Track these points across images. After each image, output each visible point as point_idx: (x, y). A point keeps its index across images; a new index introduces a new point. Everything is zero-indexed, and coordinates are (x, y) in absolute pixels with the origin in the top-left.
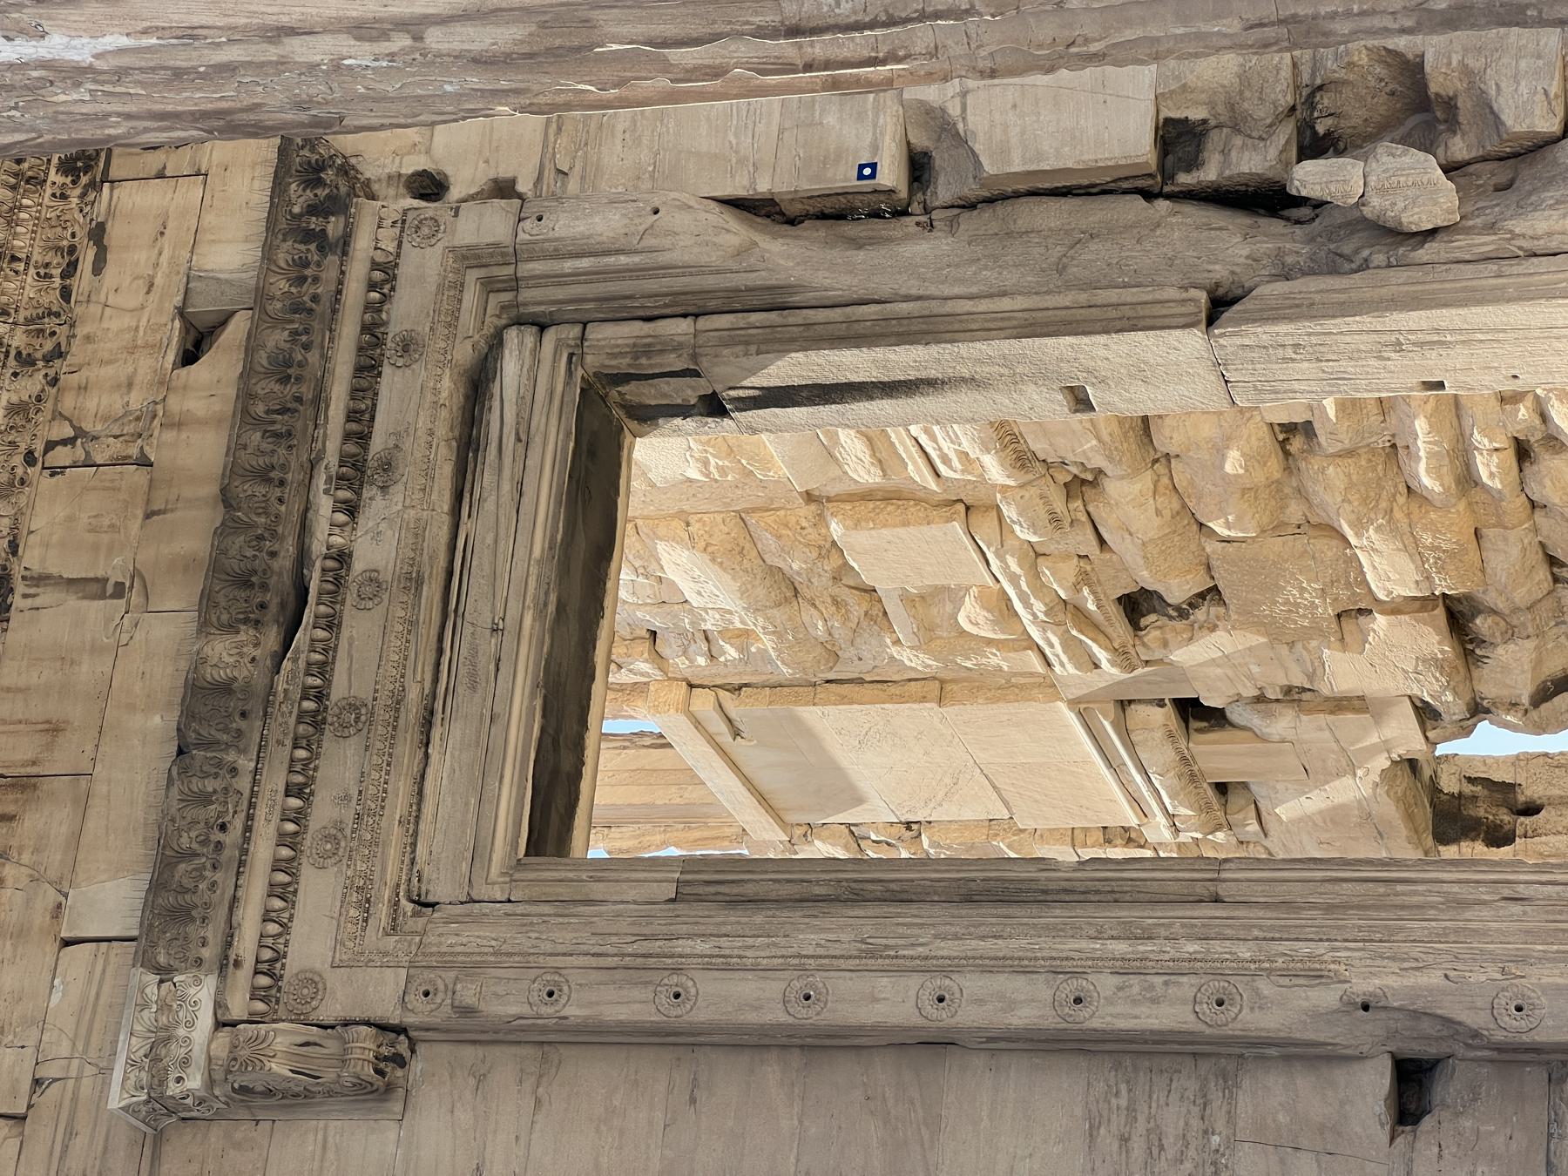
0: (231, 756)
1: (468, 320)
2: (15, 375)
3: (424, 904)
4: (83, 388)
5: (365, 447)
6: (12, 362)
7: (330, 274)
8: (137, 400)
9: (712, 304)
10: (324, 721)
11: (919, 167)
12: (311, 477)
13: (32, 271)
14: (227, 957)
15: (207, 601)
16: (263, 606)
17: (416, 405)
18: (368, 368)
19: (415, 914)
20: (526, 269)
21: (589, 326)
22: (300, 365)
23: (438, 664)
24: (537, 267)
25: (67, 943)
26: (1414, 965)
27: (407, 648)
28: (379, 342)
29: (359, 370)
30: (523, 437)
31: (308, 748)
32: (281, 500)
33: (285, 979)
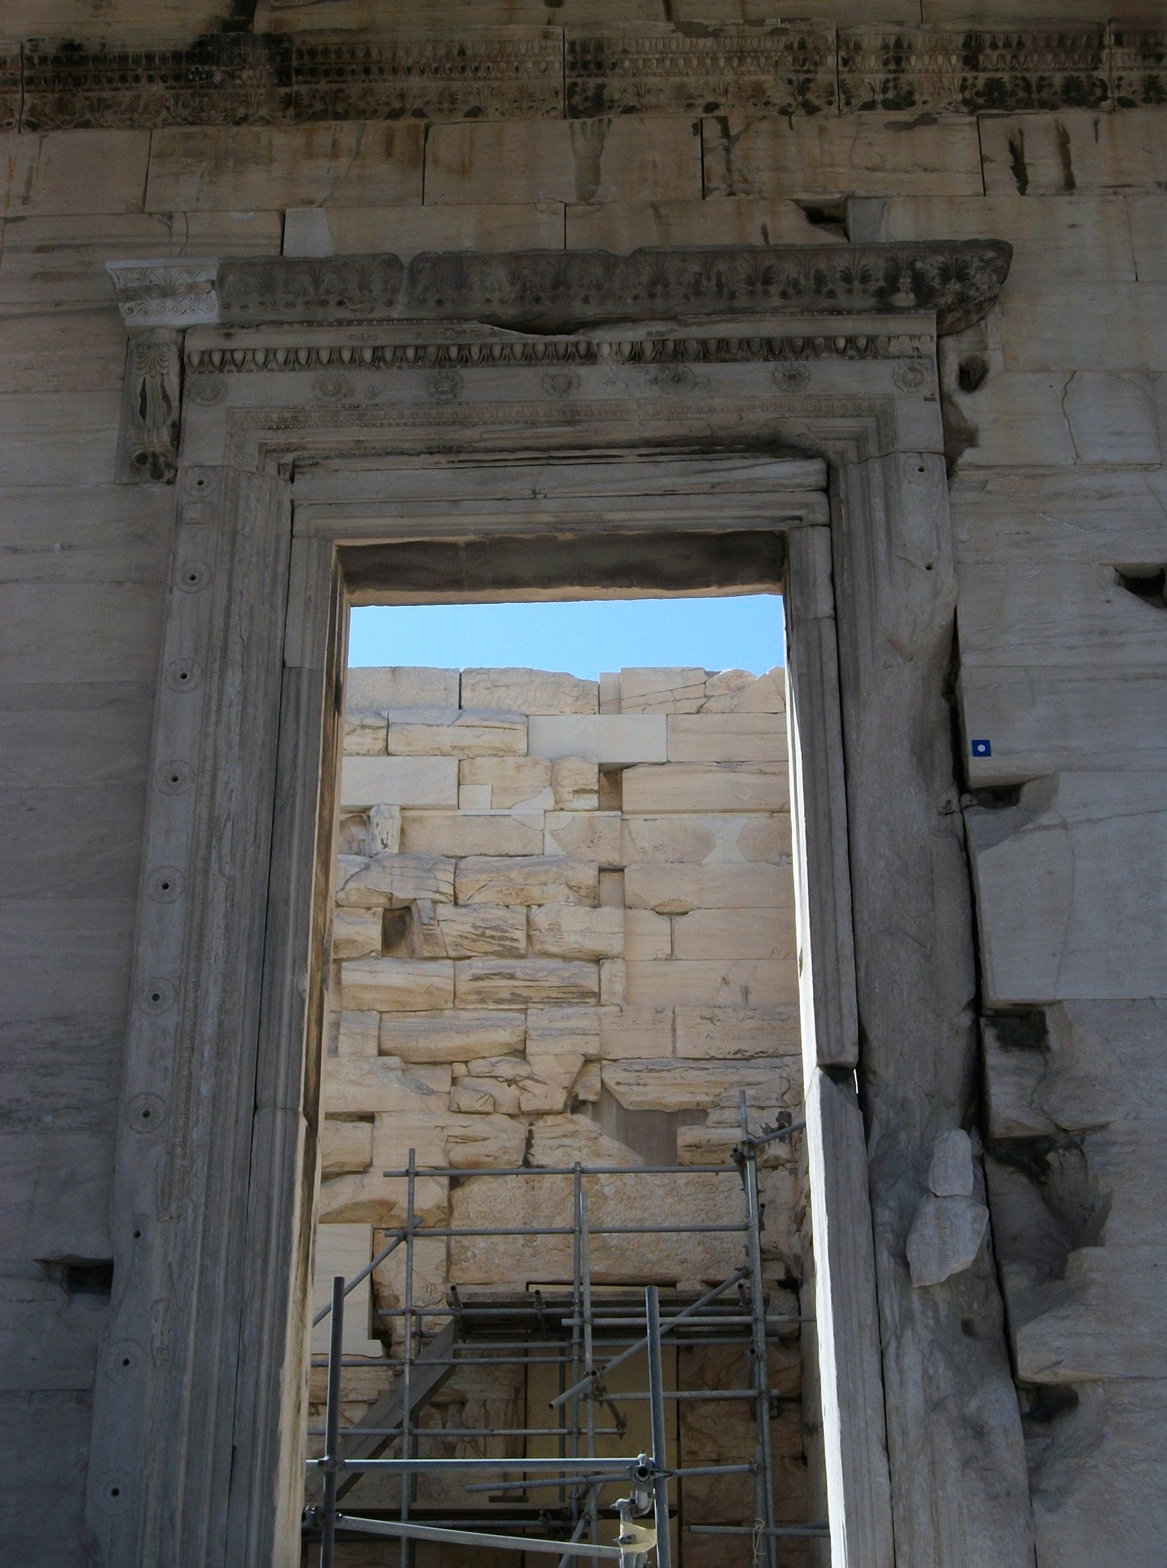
0: (402, 298)
1: (827, 423)
2: (790, 82)
3: (293, 472)
4: (776, 135)
5: (697, 359)
6: (802, 77)
7: (857, 302)
8: (764, 178)
9: (844, 628)
10: (442, 367)
11: (1004, 795)
12: (663, 320)
13: (891, 76)
14: (232, 326)
15: (537, 255)
16: (538, 300)
17: (743, 393)
18: (771, 349)
19: (280, 468)
20: (876, 467)
21: (826, 530)
22: (766, 292)
23: (502, 450)
24: (876, 475)
26: (175, 1275)
27: (509, 422)
28: (799, 353)
29: (768, 343)
30: (716, 490)
31: (417, 358)
32: (635, 298)
33: (221, 375)
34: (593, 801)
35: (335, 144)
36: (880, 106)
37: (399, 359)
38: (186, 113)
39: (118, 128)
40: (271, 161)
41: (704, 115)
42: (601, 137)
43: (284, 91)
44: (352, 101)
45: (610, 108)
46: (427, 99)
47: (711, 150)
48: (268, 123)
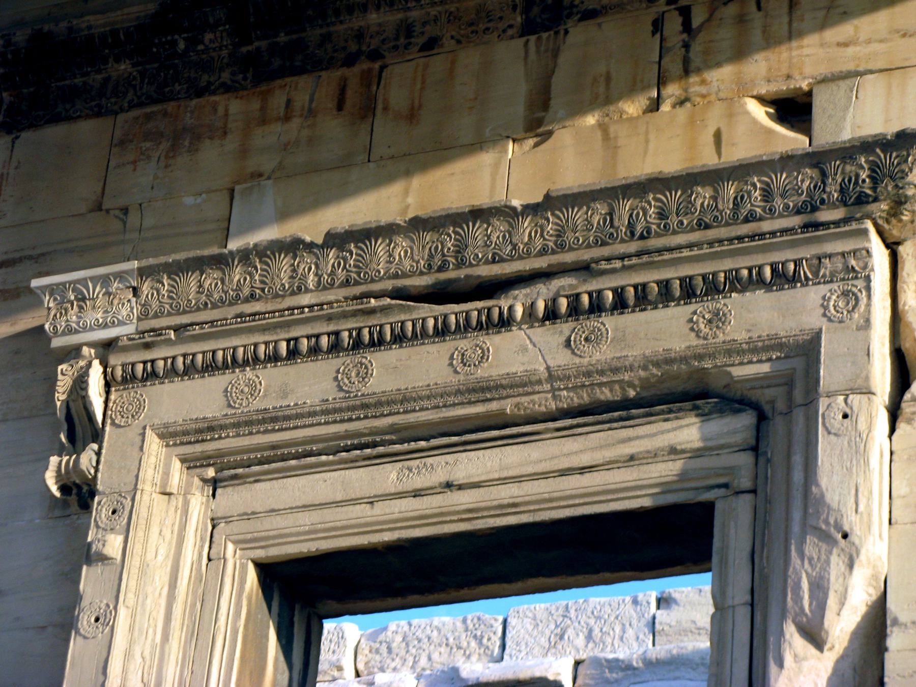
9: (758, 618)
20: (799, 415)
35: (289, 103)
37: (315, 351)
41: (666, 8)
42: (556, 53)
45: (569, 16)
46: (384, 37)
47: (669, 50)
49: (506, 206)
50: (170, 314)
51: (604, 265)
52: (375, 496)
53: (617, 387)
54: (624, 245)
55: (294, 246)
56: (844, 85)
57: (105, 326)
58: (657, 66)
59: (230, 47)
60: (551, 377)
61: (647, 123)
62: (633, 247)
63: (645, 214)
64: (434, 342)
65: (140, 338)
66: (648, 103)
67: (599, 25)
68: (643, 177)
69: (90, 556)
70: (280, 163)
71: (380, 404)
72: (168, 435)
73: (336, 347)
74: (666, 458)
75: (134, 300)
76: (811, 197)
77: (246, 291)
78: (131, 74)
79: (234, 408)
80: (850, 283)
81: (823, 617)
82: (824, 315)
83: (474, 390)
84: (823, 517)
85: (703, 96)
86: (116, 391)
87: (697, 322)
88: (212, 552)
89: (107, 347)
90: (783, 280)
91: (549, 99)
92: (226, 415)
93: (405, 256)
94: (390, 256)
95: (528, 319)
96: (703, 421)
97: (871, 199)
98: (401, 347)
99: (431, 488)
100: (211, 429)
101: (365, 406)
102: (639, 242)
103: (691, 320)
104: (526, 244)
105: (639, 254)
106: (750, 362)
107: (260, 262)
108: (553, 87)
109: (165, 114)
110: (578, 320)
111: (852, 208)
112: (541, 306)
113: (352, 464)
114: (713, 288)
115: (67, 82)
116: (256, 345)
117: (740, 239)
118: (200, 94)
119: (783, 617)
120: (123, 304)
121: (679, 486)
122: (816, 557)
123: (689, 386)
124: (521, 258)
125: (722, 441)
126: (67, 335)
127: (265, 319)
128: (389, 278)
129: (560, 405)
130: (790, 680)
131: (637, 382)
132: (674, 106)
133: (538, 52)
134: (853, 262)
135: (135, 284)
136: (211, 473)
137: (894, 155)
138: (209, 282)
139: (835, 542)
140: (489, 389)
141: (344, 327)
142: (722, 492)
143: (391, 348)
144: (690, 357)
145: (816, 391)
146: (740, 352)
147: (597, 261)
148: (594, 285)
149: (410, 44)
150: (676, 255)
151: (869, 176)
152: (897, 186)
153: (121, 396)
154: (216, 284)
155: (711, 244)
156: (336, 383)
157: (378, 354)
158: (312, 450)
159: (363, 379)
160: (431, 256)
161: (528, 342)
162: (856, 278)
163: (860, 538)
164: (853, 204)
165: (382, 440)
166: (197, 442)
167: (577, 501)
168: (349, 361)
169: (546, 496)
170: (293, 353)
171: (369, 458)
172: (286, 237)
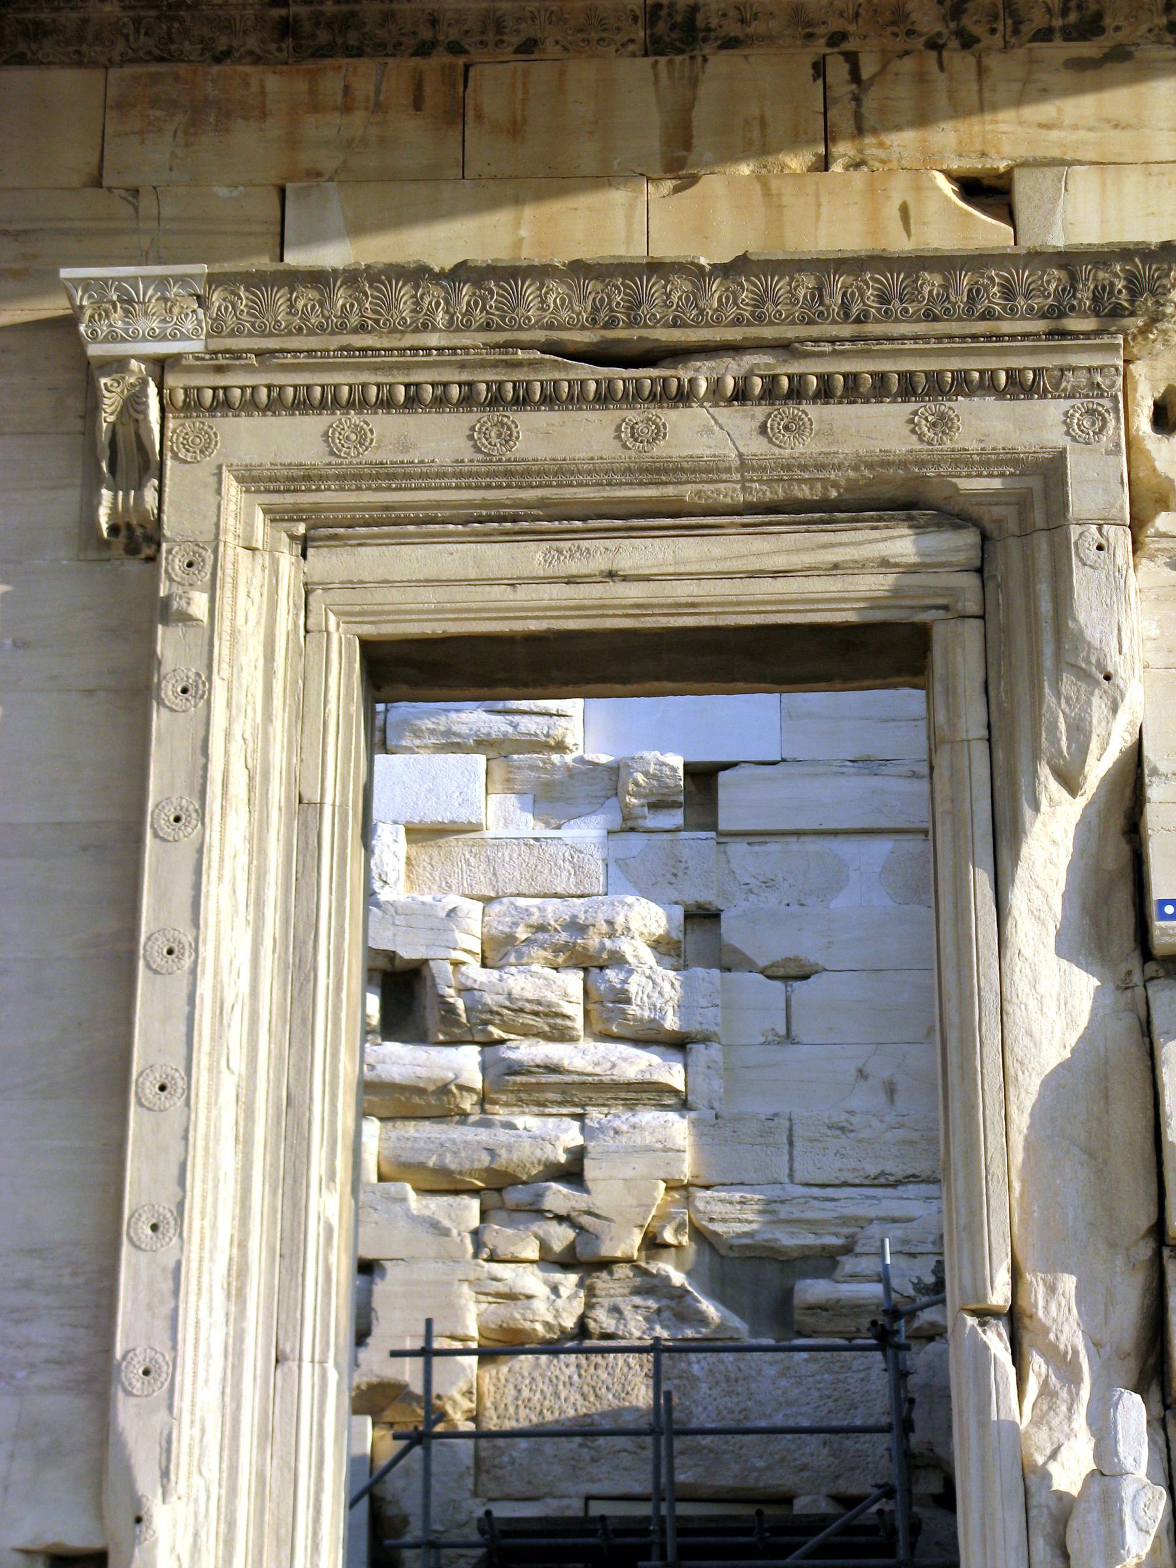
4: (921, 78)
9: (999, 755)
20: (1042, 543)
21: (977, 623)
25: (282, 192)
34: (676, 818)
35: (347, 90)
36: (1058, 35)
37: (441, 402)
38: (151, 42)
39: (63, 65)
40: (264, 116)
41: (828, 50)
42: (694, 83)
43: (277, 13)
44: (368, 29)
45: (705, 40)
46: (466, 27)
47: (836, 101)
48: (257, 60)
49: (692, 264)
50: (250, 335)
51: (809, 347)
52: (518, 578)
53: (819, 485)
54: (836, 327)
55: (418, 274)
56: (1050, 173)
57: (163, 338)
58: (821, 118)
59: (257, 7)
60: (744, 464)
61: (817, 183)
62: (847, 330)
63: (862, 295)
64: (594, 409)
65: (211, 359)
66: (814, 159)
67: (746, 57)
68: (863, 253)
69: (167, 612)
70: (344, 163)
71: (528, 473)
72: (250, 479)
73: (468, 400)
74: (874, 571)
75: (200, 311)
76: (1059, 302)
77: (354, 320)
78: (119, 19)
79: (340, 457)
80: (1095, 401)
81: (1084, 761)
82: (1068, 433)
83: (648, 471)
84: (1083, 654)
85: (883, 162)
86: (174, 418)
87: (918, 425)
88: (309, 622)
89: (161, 366)
90: (1017, 389)
91: (691, 137)
92: (330, 464)
93: (562, 305)
94: (542, 302)
95: (711, 396)
96: (917, 534)
97: (1127, 313)
98: (552, 409)
99: (590, 576)
100: (307, 478)
101: (508, 473)
102: (854, 326)
103: (912, 421)
104: (716, 310)
105: (853, 340)
106: (980, 475)
107: (371, 287)
108: (695, 123)
109: (177, 78)
110: (773, 404)
111: (1104, 319)
112: (730, 383)
113: (485, 538)
114: (936, 386)
115: (30, 15)
116: (364, 386)
117: (974, 337)
118: (219, 58)
119: (1035, 757)
120: (187, 315)
121: (891, 602)
122: (1074, 697)
123: (901, 494)
124: (708, 325)
125: (944, 559)
126: (110, 342)
127: (379, 356)
128: (542, 328)
129: (749, 498)
130: (1044, 825)
131: (843, 483)
132: (847, 168)
133: (671, 77)
134: (1099, 379)
135: (200, 292)
136: (301, 529)
137: (1154, 267)
138: (302, 303)
139: (1097, 683)
140: (666, 471)
141: (481, 378)
142: (941, 614)
143: (539, 410)
144: (911, 463)
145: (1065, 517)
146: (969, 463)
147: (802, 341)
148: (795, 368)
149: (502, 41)
150: (897, 346)
151: (1124, 287)
152: (1157, 302)
153: (183, 425)
154: (313, 307)
155: (939, 339)
156: (472, 443)
157: (523, 415)
158: (436, 515)
159: (507, 442)
160: (595, 310)
161: (713, 422)
162: (1102, 396)
163: (1125, 682)
164: (1106, 316)
165: (526, 514)
166: (288, 491)
167: (769, 608)
168: (485, 419)
169: (734, 599)
170: (413, 401)
171: (507, 533)
172: (408, 262)
